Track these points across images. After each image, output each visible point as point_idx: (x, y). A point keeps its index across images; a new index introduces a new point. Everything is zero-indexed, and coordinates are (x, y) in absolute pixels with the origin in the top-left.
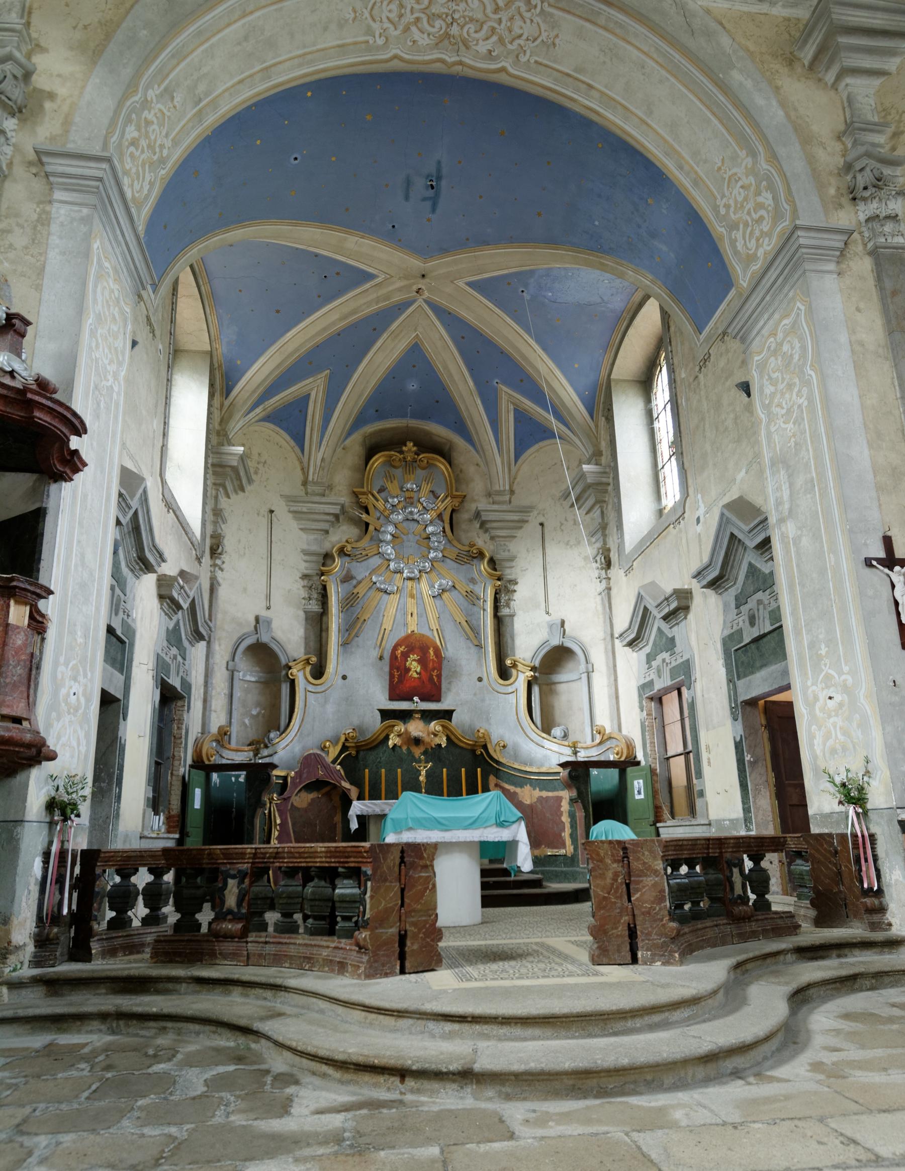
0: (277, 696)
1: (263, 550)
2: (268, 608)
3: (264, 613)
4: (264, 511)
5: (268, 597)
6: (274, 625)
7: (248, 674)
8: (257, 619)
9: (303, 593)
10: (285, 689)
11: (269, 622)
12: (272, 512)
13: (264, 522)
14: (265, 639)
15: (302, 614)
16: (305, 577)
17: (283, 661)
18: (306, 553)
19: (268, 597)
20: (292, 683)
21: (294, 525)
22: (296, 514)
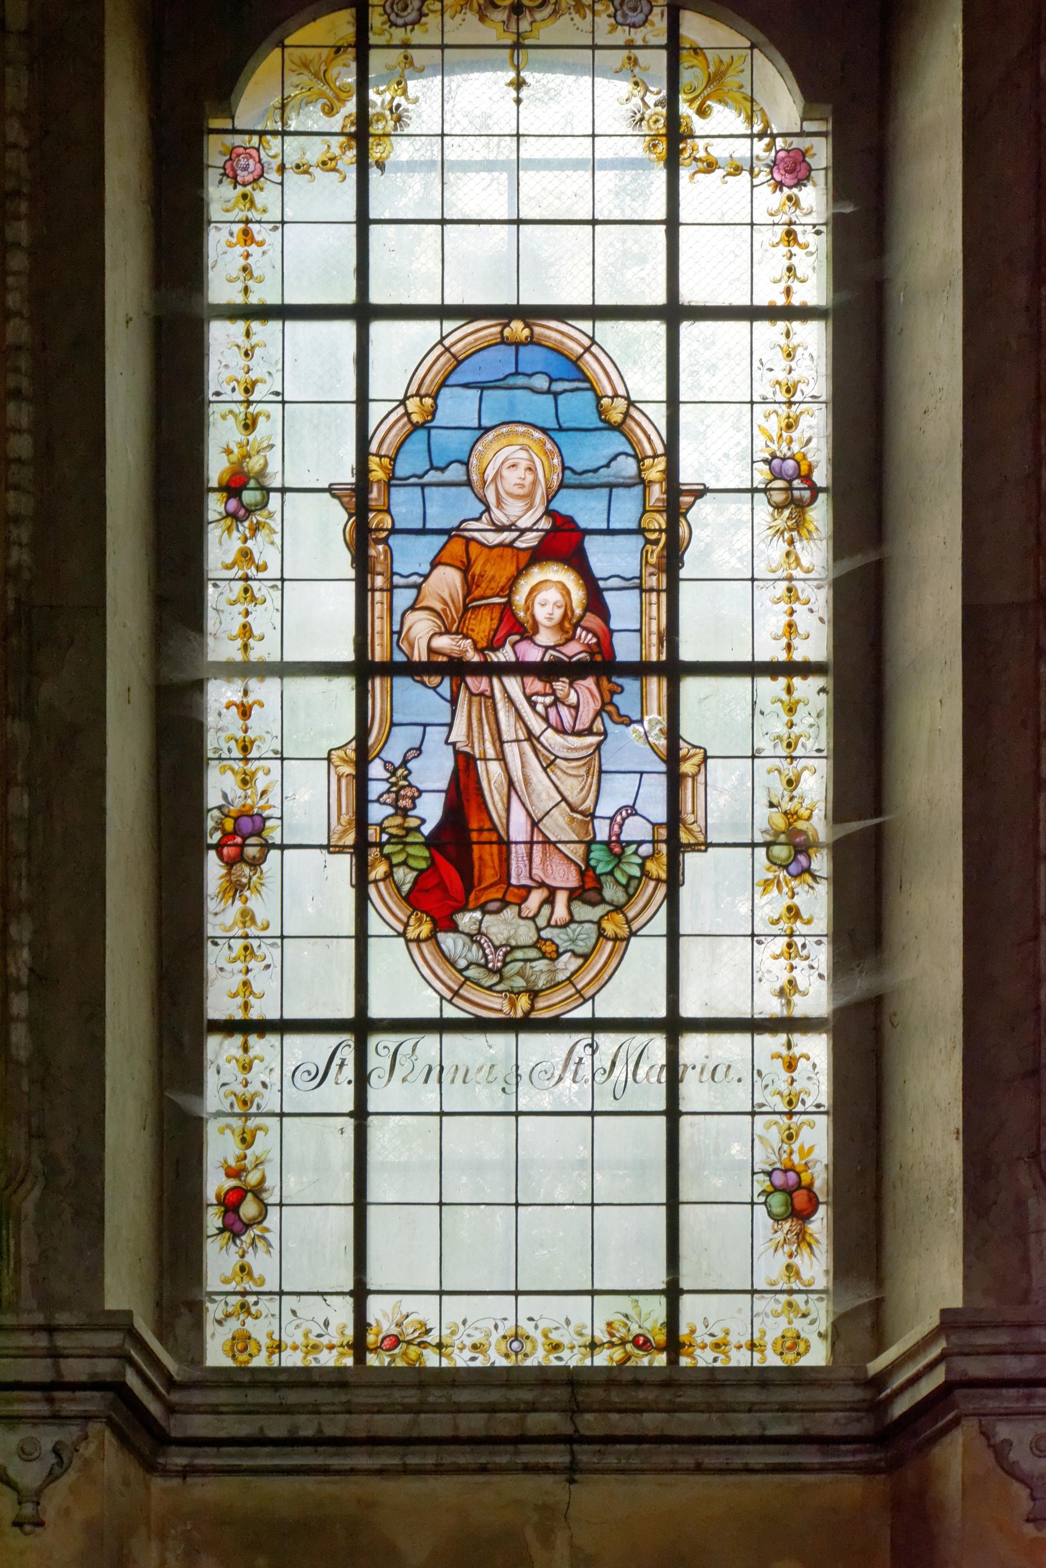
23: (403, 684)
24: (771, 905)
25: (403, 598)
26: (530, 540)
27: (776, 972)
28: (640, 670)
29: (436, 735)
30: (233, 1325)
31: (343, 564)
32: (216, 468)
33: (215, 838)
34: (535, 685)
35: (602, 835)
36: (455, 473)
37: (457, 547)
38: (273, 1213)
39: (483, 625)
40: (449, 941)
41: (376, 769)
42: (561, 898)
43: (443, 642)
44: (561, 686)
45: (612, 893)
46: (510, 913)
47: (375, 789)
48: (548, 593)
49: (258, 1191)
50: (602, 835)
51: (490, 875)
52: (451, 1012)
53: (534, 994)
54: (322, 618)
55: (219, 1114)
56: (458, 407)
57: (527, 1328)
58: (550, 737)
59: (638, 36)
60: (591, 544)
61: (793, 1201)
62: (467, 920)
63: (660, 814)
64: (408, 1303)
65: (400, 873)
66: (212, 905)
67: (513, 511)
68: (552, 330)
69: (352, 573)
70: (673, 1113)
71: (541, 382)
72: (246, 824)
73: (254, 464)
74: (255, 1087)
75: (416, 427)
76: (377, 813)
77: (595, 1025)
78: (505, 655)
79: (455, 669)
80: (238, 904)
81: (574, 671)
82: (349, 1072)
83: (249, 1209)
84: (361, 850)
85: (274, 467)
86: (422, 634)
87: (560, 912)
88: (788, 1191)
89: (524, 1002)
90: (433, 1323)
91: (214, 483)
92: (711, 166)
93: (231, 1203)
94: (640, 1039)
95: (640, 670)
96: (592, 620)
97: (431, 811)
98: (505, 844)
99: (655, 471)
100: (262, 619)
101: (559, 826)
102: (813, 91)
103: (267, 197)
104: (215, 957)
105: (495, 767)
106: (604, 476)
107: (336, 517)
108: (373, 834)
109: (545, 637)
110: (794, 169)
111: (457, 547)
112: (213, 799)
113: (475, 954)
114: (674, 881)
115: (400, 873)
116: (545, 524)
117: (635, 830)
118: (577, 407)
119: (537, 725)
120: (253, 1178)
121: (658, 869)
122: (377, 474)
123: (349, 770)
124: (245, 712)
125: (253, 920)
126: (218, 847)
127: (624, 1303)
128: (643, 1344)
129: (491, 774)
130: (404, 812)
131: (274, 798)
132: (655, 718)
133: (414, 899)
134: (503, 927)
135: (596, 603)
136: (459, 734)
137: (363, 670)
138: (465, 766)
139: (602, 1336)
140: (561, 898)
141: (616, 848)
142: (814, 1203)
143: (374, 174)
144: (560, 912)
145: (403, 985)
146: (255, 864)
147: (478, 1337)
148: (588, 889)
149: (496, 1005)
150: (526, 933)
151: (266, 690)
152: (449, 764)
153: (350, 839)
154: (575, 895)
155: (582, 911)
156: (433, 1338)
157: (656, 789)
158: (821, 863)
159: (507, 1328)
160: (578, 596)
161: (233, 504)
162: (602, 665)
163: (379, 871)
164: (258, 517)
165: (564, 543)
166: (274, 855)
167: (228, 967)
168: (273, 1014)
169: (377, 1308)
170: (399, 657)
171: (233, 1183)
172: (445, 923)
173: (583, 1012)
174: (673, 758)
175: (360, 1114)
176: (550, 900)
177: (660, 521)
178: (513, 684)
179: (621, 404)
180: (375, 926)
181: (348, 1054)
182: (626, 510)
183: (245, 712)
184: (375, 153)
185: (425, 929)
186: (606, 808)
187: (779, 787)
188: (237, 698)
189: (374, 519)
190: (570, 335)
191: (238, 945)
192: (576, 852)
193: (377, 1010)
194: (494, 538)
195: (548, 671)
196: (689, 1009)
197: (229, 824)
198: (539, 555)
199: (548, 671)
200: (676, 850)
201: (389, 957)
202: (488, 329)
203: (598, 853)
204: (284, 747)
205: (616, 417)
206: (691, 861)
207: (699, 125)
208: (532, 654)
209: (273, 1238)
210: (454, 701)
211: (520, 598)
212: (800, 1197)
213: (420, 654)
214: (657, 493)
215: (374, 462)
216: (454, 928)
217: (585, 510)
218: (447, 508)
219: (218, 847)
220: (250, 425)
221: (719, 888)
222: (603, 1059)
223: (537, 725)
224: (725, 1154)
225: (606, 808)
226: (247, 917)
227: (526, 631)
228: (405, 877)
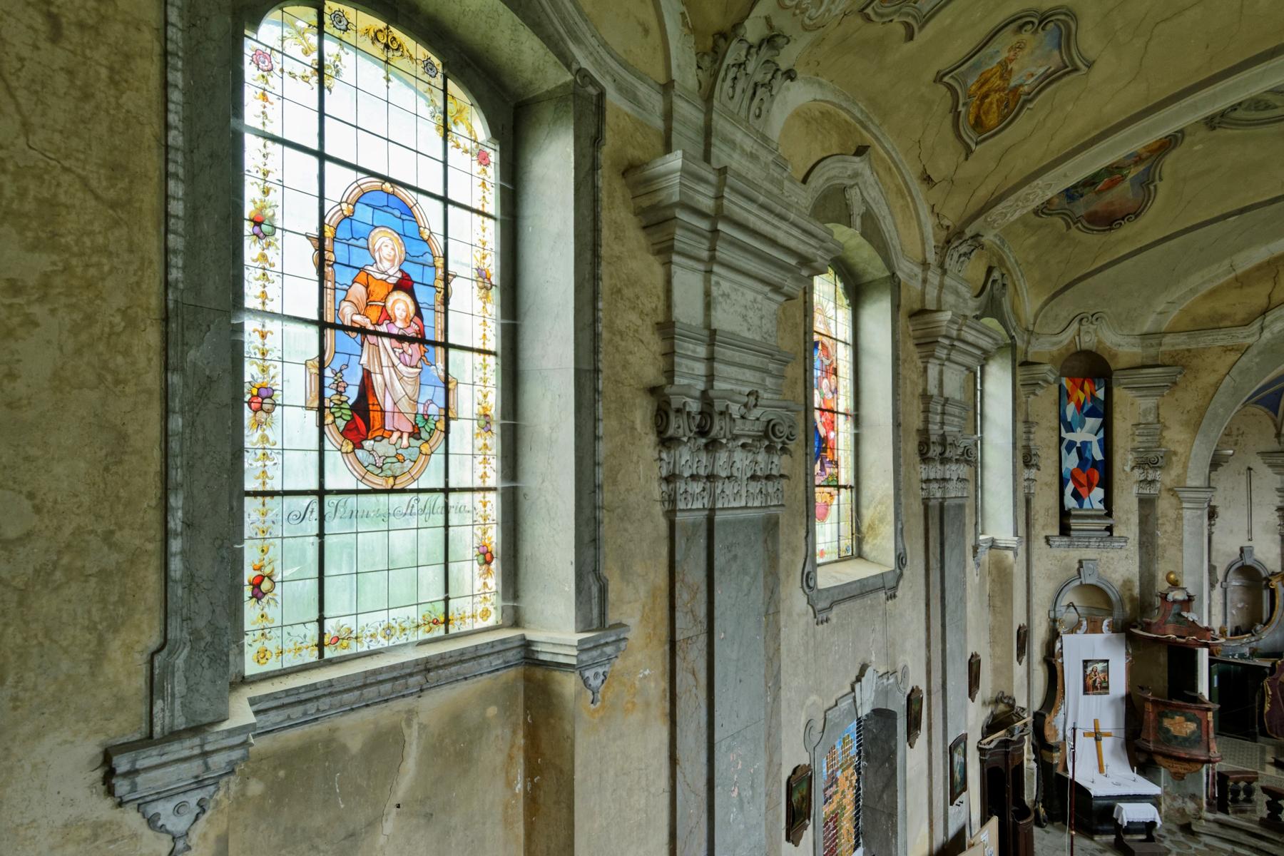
0: (1260, 597)
1: (1244, 499)
2: (1250, 540)
3: (1247, 544)
4: (1244, 469)
5: (1250, 531)
6: (1256, 551)
7: (1235, 582)
8: (1242, 549)
9: (1278, 521)
10: (1266, 595)
11: (1251, 552)
12: (1250, 469)
13: (1244, 478)
14: (1249, 562)
15: (1278, 537)
16: (1279, 509)
17: (1264, 575)
18: (1278, 490)
19: (1250, 531)
20: (1273, 592)
21: (1269, 471)
22: (1271, 466)
23: (340, 333)
24: (480, 442)
25: (340, 295)
26: (393, 280)
27: (480, 470)
28: (435, 344)
29: (354, 359)
30: (257, 646)
31: (313, 272)
32: (249, 210)
33: (247, 399)
34: (395, 343)
35: (421, 411)
36: (362, 242)
37: (363, 276)
38: (278, 586)
39: (374, 313)
40: (359, 453)
41: (328, 372)
42: (405, 436)
43: (357, 318)
44: (406, 345)
45: (424, 435)
46: (385, 441)
47: (328, 382)
48: (400, 304)
49: (270, 577)
50: (421, 411)
51: (377, 425)
52: (361, 486)
53: (395, 477)
54: (302, 297)
55: (251, 538)
56: (364, 213)
57: (392, 623)
58: (401, 367)
59: (433, 81)
60: (416, 286)
61: (486, 558)
62: (368, 444)
63: (442, 404)
64: (343, 621)
65: (339, 421)
66: (246, 432)
67: (385, 265)
68: (401, 192)
69: (317, 278)
70: (447, 527)
71: (397, 213)
72: (264, 393)
73: (269, 212)
74: (269, 524)
75: (346, 217)
76: (329, 393)
77: (419, 491)
78: (383, 329)
79: (363, 331)
80: (260, 432)
81: (411, 340)
82: (316, 515)
83: (266, 585)
84: (321, 409)
85: (278, 216)
86: (349, 314)
87: (405, 442)
88: (484, 554)
89: (391, 480)
90: (354, 628)
91: (246, 216)
92: (458, 147)
93: (256, 585)
94: (435, 495)
95: (435, 344)
96: (417, 319)
97: (352, 394)
98: (383, 412)
99: (440, 263)
100: (273, 291)
101: (405, 406)
102: (496, 132)
103: (274, 80)
104: (249, 460)
105: (379, 377)
106: (421, 260)
107: (310, 250)
108: (327, 403)
109: (399, 324)
110: (483, 160)
111: (363, 276)
112: (247, 378)
113: (371, 460)
114: (447, 431)
115: (339, 421)
116: (399, 275)
117: (433, 410)
118: (410, 228)
119: (396, 361)
120: (267, 571)
121: (441, 426)
122: (329, 233)
123: (316, 371)
124: (263, 336)
125: (268, 440)
126: (249, 403)
127: (429, 607)
128: (436, 622)
129: (377, 380)
130: (340, 394)
131: (278, 379)
132: (441, 366)
133: (345, 434)
134: (383, 448)
135: (418, 313)
136: (364, 360)
137: (322, 325)
138: (367, 375)
139: (421, 622)
140: (405, 436)
141: (426, 418)
142: (492, 558)
143: (326, 91)
144: (405, 442)
145: (340, 475)
146: (268, 412)
147: (373, 631)
148: (415, 434)
149: (380, 483)
150: (392, 452)
151: (274, 326)
152: (360, 374)
153: (316, 404)
154: (411, 435)
155: (414, 442)
156: (354, 635)
157: (441, 392)
158: (496, 428)
159: (385, 625)
160: (412, 308)
161: (257, 229)
162: (420, 339)
163: (329, 419)
164: (270, 239)
165: (405, 285)
166: (278, 409)
167: (255, 464)
168: (278, 488)
169: (329, 625)
170: (338, 322)
171: (258, 573)
172: (358, 445)
173: (414, 486)
174: (446, 382)
175: (321, 535)
176: (401, 437)
177: (441, 284)
178: (386, 341)
179: (427, 232)
180: (328, 446)
181: (316, 506)
182: (429, 276)
183: (263, 336)
184: (327, 83)
185: (350, 447)
186: (422, 400)
187: (481, 398)
188: (260, 328)
189: (327, 255)
190: (409, 196)
191: (260, 452)
192: (411, 417)
193: (328, 486)
194: (379, 276)
195: (401, 338)
196: (451, 485)
197: (255, 392)
198: (398, 287)
199: (401, 338)
200: (447, 419)
201: (332, 457)
202: (376, 183)
203: (419, 418)
204: (279, 353)
205: (426, 237)
206: (452, 423)
207: (454, 129)
208: (395, 331)
209: (279, 600)
210: (362, 345)
211: (389, 304)
212: (488, 556)
213: (347, 322)
214: (440, 272)
215: (327, 228)
216: (362, 447)
217: (415, 273)
218: (358, 258)
219: (249, 403)
220: (266, 192)
221: (463, 433)
222: (421, 505)
223: (396, 361)
224: (466, 540)
225: (422, 400)
226: (265, 438)
227: (391, 320)
228: (341, 423)
